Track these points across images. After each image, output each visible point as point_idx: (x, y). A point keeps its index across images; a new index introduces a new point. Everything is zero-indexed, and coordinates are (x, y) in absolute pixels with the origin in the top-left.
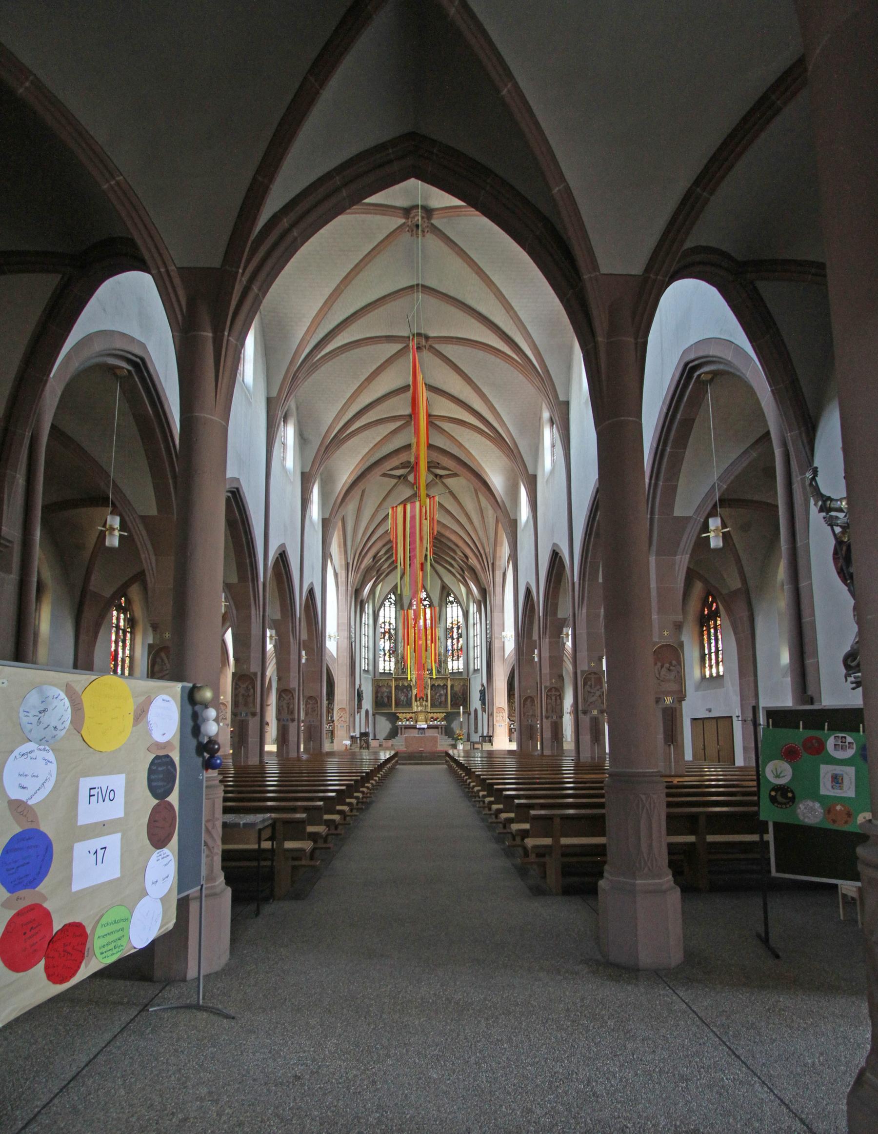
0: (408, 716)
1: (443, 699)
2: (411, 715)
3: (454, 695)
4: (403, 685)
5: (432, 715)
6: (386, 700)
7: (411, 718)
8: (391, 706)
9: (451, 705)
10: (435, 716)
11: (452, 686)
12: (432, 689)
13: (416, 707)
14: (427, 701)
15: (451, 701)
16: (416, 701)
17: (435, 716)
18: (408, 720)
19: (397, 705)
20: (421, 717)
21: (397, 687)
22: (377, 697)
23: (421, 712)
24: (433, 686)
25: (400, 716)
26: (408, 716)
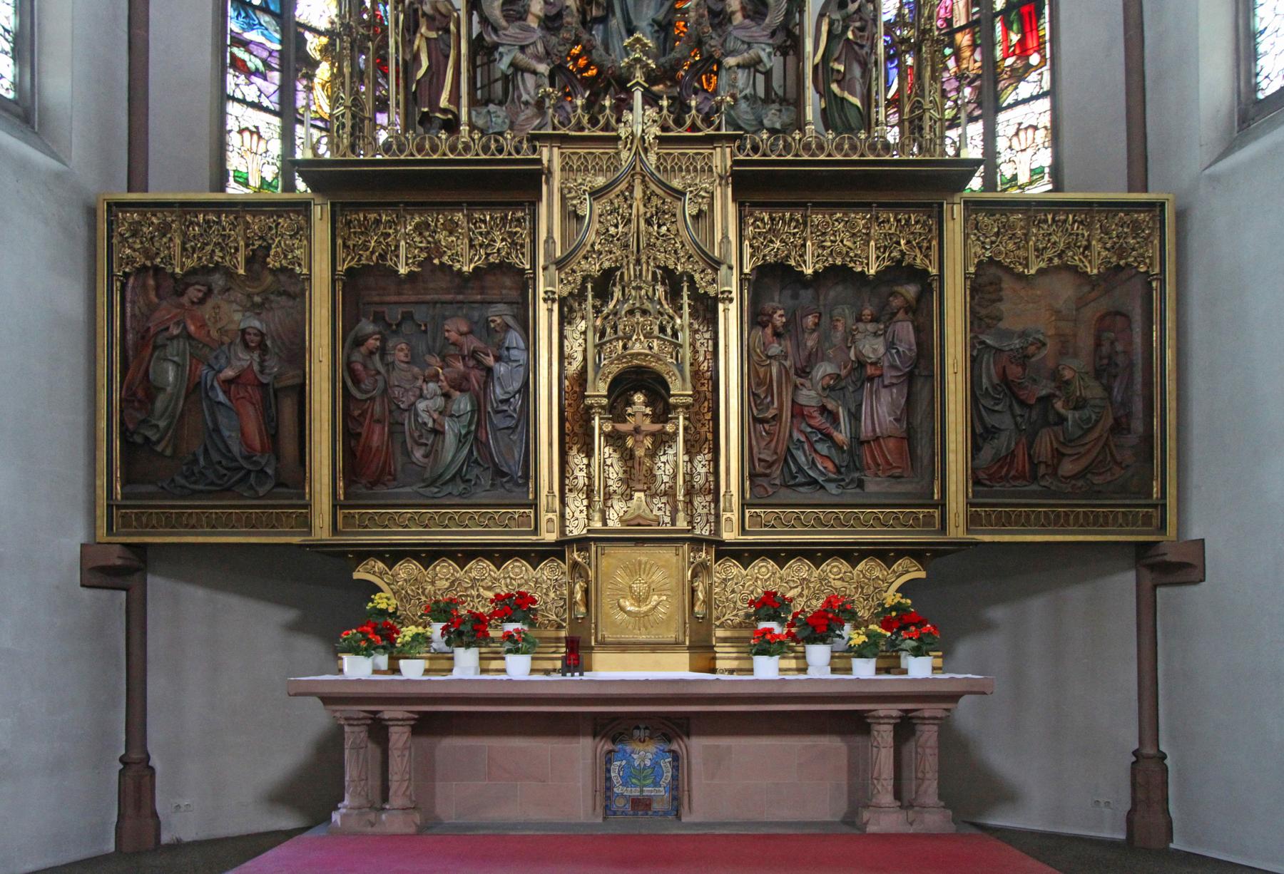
0: (483, 584)
1: (881, 411)
2: (517, 576)
3: (1005, 385)
4: (432, 269)
5: (763, 576)
6: (241, 428)
7: (517, 605)
8: (295, 478)
9: (976, 479)
10: (802, 585)
11: (984, 285)
12: (756, 318)
13: (573, 493)
14: (704, 439)
15: (979, 436)
16: (575, 433)
17: (802, 585)
18: (469, 631)
19: (361, 470)
20: (644, 589)
21: (356, 287)
22: (137, 394)
23: (638, 536)
24: (770, 279)
25: (390, 587)
26: (483, 584)
